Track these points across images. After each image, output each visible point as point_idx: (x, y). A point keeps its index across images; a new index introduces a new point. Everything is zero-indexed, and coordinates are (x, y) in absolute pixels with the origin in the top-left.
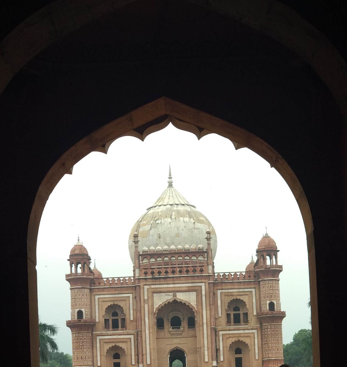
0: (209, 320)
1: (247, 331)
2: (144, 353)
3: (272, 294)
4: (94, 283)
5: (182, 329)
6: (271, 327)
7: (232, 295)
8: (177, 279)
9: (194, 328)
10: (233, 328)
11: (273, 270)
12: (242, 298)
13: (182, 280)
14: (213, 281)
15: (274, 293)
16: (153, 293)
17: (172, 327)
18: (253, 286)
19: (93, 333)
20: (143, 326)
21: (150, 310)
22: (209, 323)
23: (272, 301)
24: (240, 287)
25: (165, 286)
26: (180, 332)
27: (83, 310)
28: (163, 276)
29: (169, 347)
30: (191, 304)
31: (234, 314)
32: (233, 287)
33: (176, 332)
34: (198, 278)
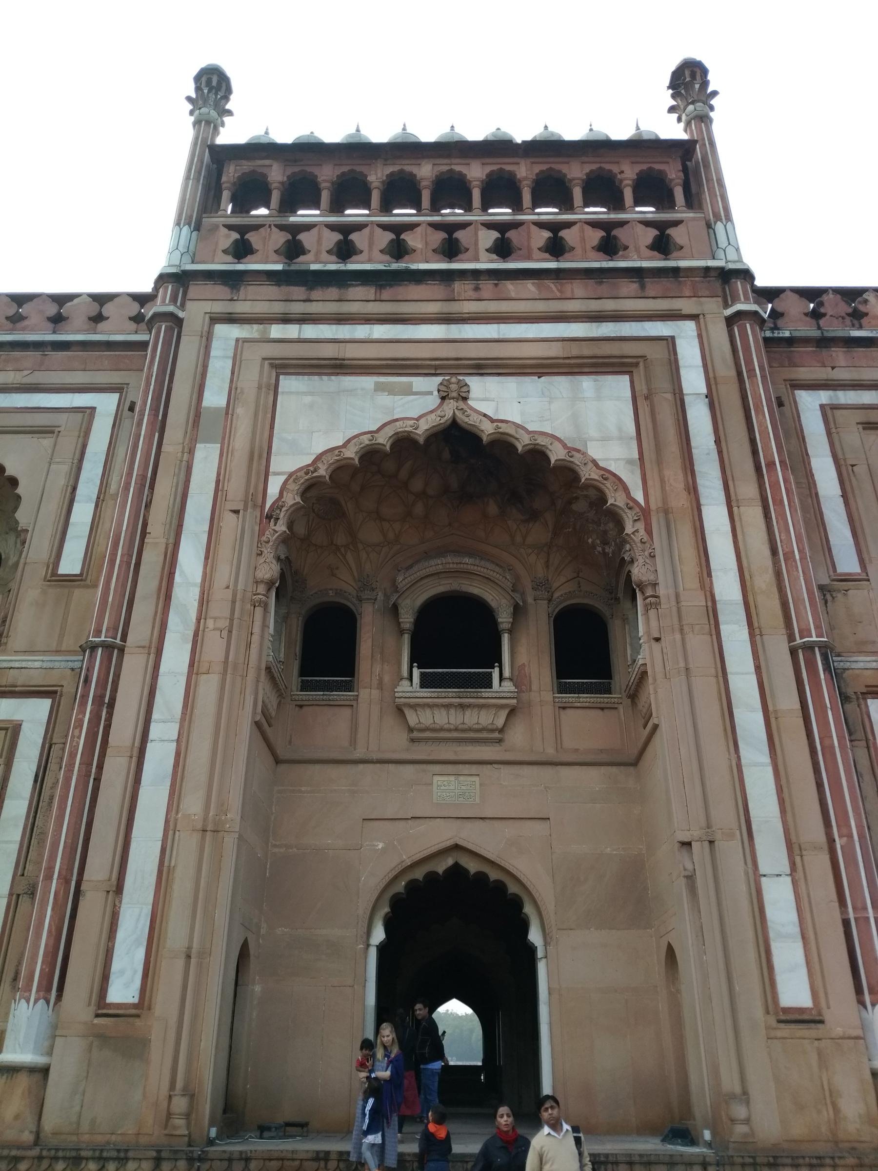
0: (764, 580)
2: (99, 867)
5: (508, 686)
8: (477, 289)
9: (607, 690)
13: (513, 295)
16: (283, 367)
17: (423, 676)
20: (143, 610)
21: (235, 488)
25: (380, 331)
26: (485, 718)
28: (368, 267)
29: (381, 846)
30: (595, 451)
33: (455, 718)
34: (643, 287)
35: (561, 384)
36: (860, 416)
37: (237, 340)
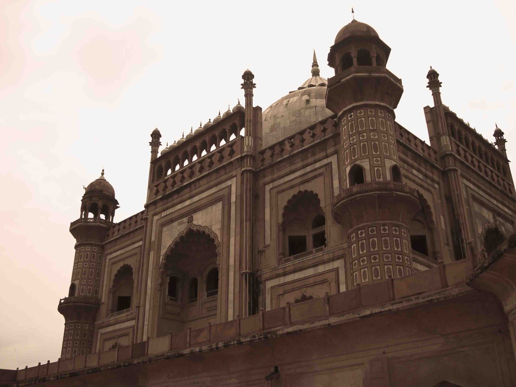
1: (321, 269)
3: (355, 146)
4: (108, 235)
6: (357, 235)
7: (292, 187)
10: (292, 268)
11: (347, 80)
12: (309, 187)
14: (251, 167)
15: (361, 141)
16: (163, 225)
18: (330, 150)
19: (96, 323)
22: (238, 264)
23: (358, 162)
24: (305, 162)
25: (179, 207)
27: (77, 282)
31: (315, 237)
32: (293, 167)
34: (226, 169)
35: (209, 208)
36: (275, 190)
37: (157, 220)
